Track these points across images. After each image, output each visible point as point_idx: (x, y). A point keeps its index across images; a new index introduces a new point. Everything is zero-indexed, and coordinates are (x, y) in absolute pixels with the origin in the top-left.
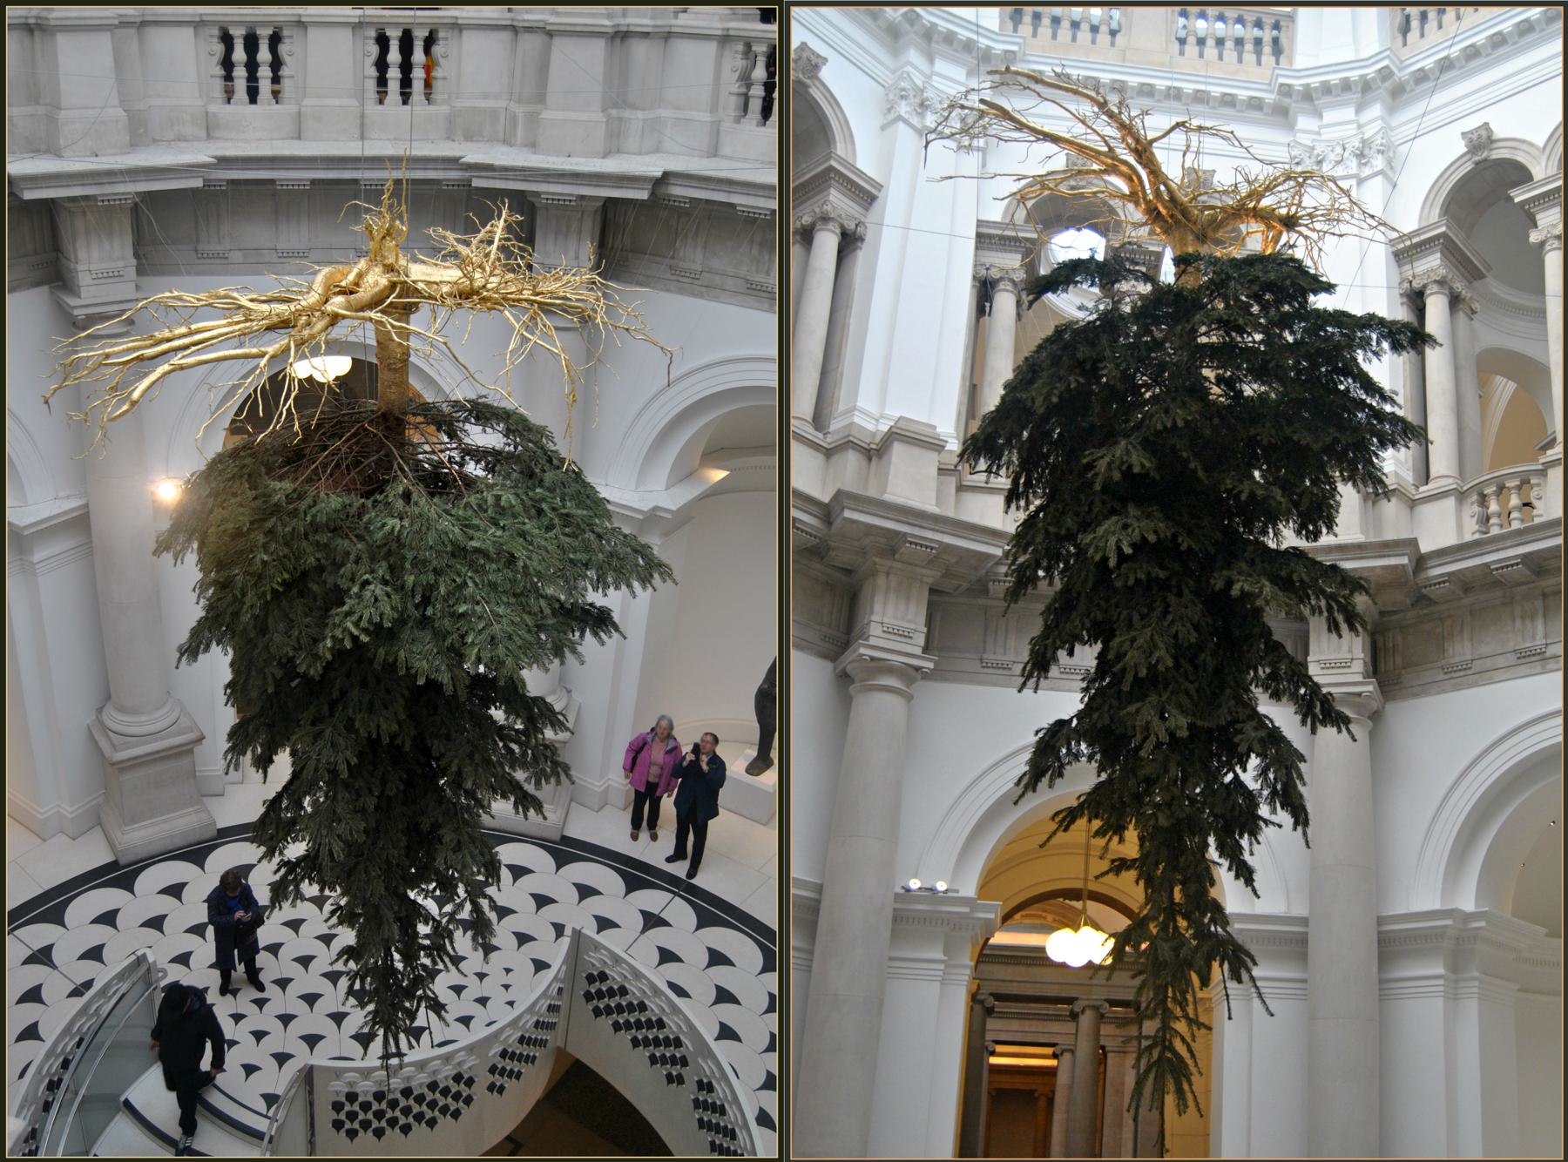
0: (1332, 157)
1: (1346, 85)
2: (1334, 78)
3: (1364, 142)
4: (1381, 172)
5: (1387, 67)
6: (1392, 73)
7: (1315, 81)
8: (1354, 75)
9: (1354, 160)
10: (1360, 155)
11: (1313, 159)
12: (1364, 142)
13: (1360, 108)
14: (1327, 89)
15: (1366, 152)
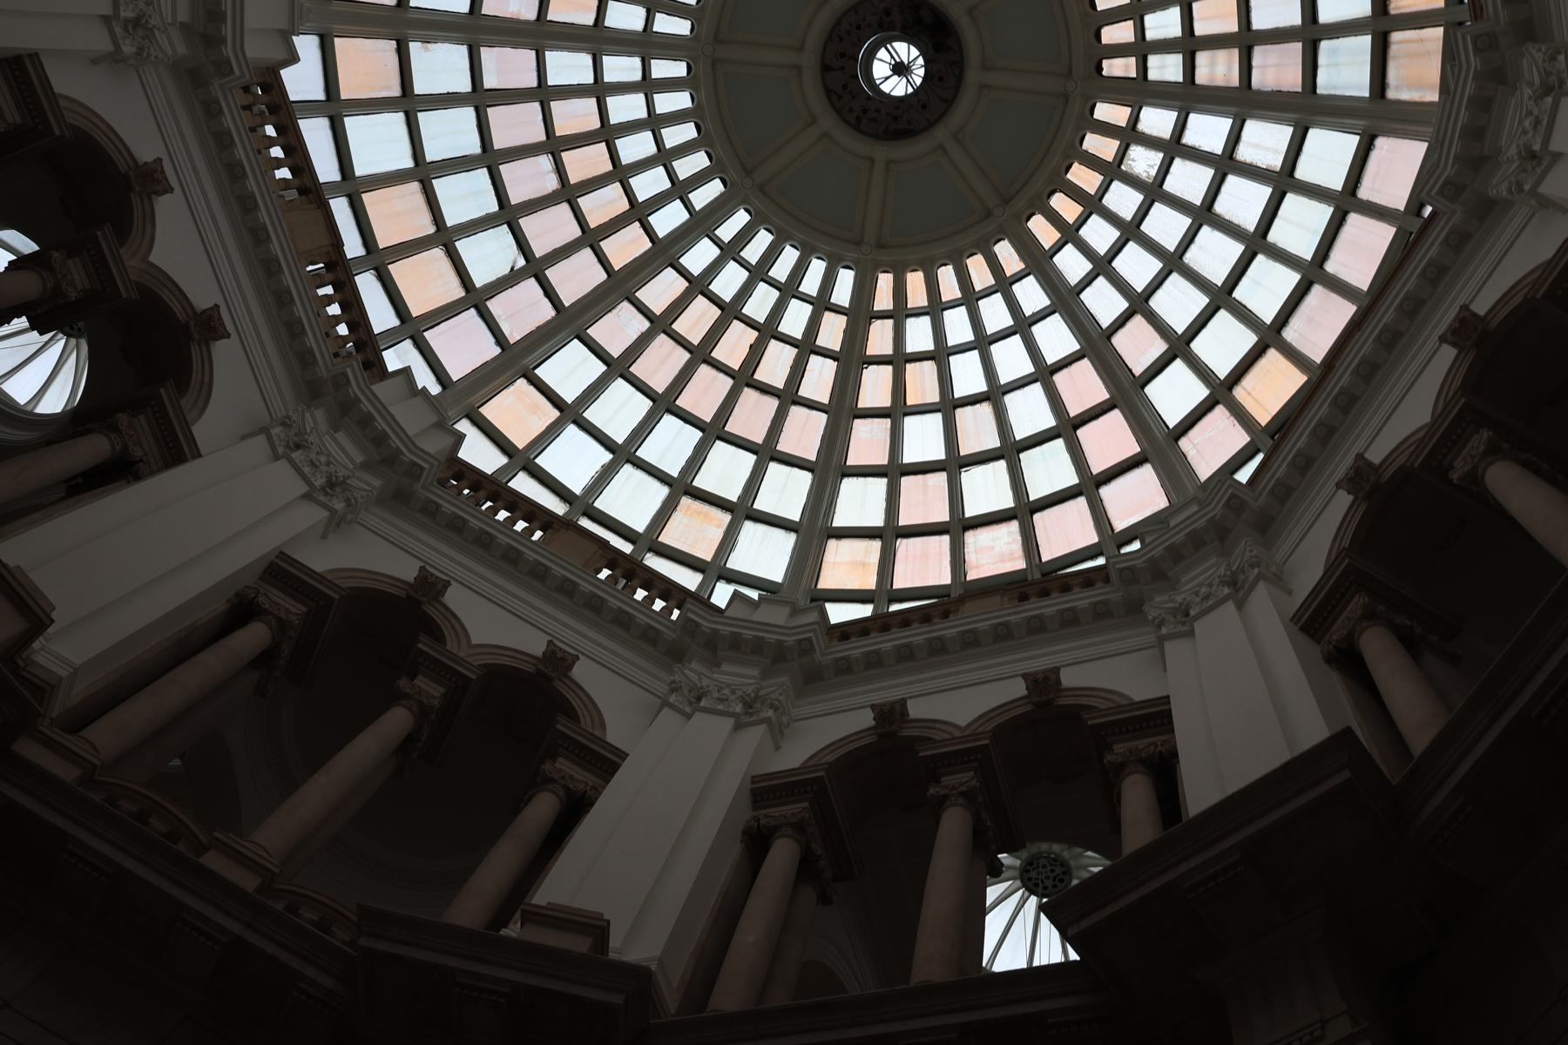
0: (313, 456)
1: (380, 440)
2: (381, 424)
3: (343, 482)
4: (333, 511)
5: (422, 469)
6: (419, 477)
7: (366, 406)
8: (395, 441)
9: (324, 480)
10: (332, 484)
11: (296, 439)
12: (343, 482)
13: (365, 466)
14: (366, 421)
15: (338, 490)
